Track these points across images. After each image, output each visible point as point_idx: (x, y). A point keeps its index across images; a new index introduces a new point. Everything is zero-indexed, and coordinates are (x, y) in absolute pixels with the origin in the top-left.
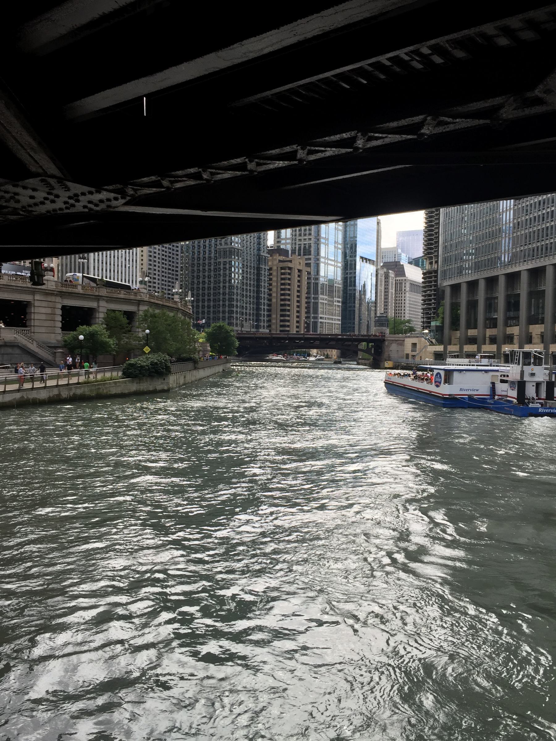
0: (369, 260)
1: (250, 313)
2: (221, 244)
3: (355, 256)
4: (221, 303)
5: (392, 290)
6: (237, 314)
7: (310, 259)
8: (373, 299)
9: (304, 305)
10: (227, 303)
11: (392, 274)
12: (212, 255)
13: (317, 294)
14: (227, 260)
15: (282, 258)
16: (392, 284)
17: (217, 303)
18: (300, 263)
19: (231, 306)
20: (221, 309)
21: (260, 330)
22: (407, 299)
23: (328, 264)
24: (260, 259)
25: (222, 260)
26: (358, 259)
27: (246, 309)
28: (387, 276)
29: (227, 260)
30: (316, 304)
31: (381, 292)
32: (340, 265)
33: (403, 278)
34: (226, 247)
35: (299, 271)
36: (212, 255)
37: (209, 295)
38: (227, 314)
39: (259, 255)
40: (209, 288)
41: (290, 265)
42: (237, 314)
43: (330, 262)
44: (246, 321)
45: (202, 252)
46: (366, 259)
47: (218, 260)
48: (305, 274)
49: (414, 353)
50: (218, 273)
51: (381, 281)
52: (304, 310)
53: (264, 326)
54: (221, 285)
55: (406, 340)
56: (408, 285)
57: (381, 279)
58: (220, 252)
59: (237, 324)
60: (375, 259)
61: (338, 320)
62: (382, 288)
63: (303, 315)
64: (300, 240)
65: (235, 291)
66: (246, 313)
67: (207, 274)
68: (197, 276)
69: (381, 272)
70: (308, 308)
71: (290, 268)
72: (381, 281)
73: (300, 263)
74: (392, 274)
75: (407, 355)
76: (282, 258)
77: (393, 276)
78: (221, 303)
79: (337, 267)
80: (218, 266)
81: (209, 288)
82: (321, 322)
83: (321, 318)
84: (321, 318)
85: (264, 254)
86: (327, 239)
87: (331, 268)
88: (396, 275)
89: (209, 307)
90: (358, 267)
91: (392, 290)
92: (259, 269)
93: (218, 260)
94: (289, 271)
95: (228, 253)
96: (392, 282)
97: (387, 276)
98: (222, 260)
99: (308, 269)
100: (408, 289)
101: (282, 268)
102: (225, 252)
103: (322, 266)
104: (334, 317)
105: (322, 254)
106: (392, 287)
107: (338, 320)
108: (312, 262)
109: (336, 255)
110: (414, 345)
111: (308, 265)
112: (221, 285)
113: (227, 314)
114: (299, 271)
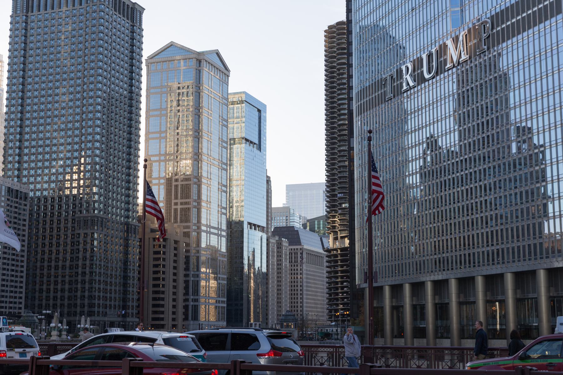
0: (259, 226)
2: (81, 212)
4: (79, 286)
5: (286, 263)
6: (99, 300)
7: (188, 227)
8: (264, 270)
9: (181, 285)
14: (89, 232)
16: (286, 255)
21: (128, 319)
23: (211, 233)
25: (82, 232)
27: (111, 293)
28: (279, 246)
31: (273, 265)
32: (224, 233)
33: (299, 247)
36: (70, 225)
38: (86, 300)
39: (127, 224)
40: (64, 267)
42: (99, 300)
43: (212, 230)
44: (110, 308)
45: (55, 221)
46: (255, 225)
47: (77, 232)
51: (273, 252)
54: (80, 263)
57: (273, 249)
58: (79, 222)
59: (98, 312)
60: (265, 225)
61: (223, 302)
63: (181, 297)
66: (111, 298)
70: (186, 288)
72: (273, 252)
74: (285, 242)
77: (287, 245)
79: (221, 236)
80: (76, 239)
81: (64, 267)
88: (290, 244)
89: (63, 290)
90: (245, 235)
91: (286, 263)
92: (127, 240)
93: (77, 232)
95: (89, 223)
96: (286, 252)
97: (279, 246)
98: (82, 232)
99: (187, 240)
102: (86, 222)
103: (204, 235)
105: (204, 221)
106: (286, 259)
107: (223, 302)
111: (187, 235)
113: (86, 300)
114: (176, 242)
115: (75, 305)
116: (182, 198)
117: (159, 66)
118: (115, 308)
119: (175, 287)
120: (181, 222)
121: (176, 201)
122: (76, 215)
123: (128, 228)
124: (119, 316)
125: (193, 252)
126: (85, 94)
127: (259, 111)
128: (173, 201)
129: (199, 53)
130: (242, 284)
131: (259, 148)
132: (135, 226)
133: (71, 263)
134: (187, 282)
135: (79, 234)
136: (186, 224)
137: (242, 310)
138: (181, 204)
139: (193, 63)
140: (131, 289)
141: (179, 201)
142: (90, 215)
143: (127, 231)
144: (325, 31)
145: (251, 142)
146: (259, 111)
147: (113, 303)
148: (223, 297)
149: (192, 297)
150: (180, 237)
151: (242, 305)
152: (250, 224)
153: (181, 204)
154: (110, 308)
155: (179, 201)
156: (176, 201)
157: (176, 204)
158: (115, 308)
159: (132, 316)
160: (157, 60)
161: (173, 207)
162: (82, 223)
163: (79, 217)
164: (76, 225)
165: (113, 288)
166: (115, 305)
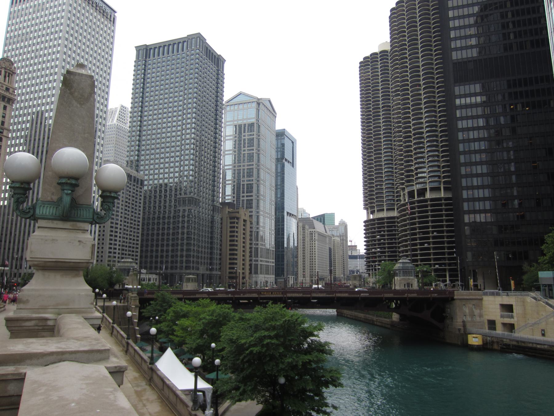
0: (293, 215)
1: (204, 257)
2: (180, 194)
3: (283, 212)
5: (307, 239)
6: (193, 258)
7: (251, 212)
9: (248, 250)
10: (185, 248)
11: (307, 227)
12: (173, 203)
13: (258, 240)
15: (231, 210)
17: (175, 248)
18: (245, 214)
19: (188, 250)
20: (179, 253)
22: (316, 245)
24: (214, 209)
25: (181, 209)
26: (285, 214)
27: (202, 253)
28: (304, 228)
29: (187, 208)
30: (257, 249)
32: (273, 218)
33: (313, 230)
34: (185, 196)
35: (245, 221)
36: (173, 203)
37: (168, 240)
39: (214, 206)
40: (168, 234)
41: (237, 215)
42: (193, 258)
44: (201, 264)
46: (290, 214)
47: (178, 208)
48: (248, 223)
49: (507, 321)
50: (177, 219)
52: (248, 254)
53: (216, 269)
55: (485, 298)
56: (316, 235)
58: (179, 201)
61: (273, 262)
62: (301, 237)
64: (243, 197)
65: (193, 237)
66: (202, 257)
67: (166, 221)
68: (158, 223)
69: (301, 224)
70: (251, 252)
71: (238, 218)
73: (245, 214)
75: (492, 324)
76: (231, 210)
78: (179, 248)
80: (177, 214)
82: (261, 265)
83: (261, 261)
84: (261, 261)
85: (218, 205)
86: (264, 197)
87: (268, 221)
90: (285, 220)
93: (178, 208)
94: (236, 221)
95: (187, 202)
97: (304, 228)
98: (181, 209)
100: (316, 238)
101: (231, 218)
104: (270, 260)
105: (261, 208)
107: (273, 262)
108: (254, 214)
109: (271, 210)
110: (508, 308)
112: (180, 231)
114: (245, 221)
115: (177, 262)
116: (247, 193)
117: (232, 108)
118: (204, 264)
119: (244, 251)
120: (246, 208)
121: (243, 195)
122: (178, 197)
123: (213, 208)
124: (207, 270)
125: (254, 230)
126: (185, 111)
127: (293, 142)
128: (241, 195)
129: (259, 99)
130: (284, 251)
131: (293, 166)
132: (218, 207)
133: (174, 231)
134: (251, 248)
135: (179, 210)
136: (250, 210)
137: (284, 268)
138: (247, 196)
139: (254, 105)
140: (215, 251)
141: (245, 194)
142: (187, 196)
143: (213, 210)
144: (361, 63)
145: (288, 162)
146: (293, 142)
147: (203, 261)
148: (273, 259)
149: (254, 259)
150: (247, 218)
151: (284, 265)
152: (288, 213)
153: (247, 196)
154: (201, 264)
155: (245, 194)
156: (243, 195)
157: (243, 197)
158: (204, 264)
159: (216, 270)
160: (231, 104)
161: (241, 199)
162: (181, 202)
163: (180, 198)
164: (177, 204)
165: (203, 250)
166: (204, 262)
